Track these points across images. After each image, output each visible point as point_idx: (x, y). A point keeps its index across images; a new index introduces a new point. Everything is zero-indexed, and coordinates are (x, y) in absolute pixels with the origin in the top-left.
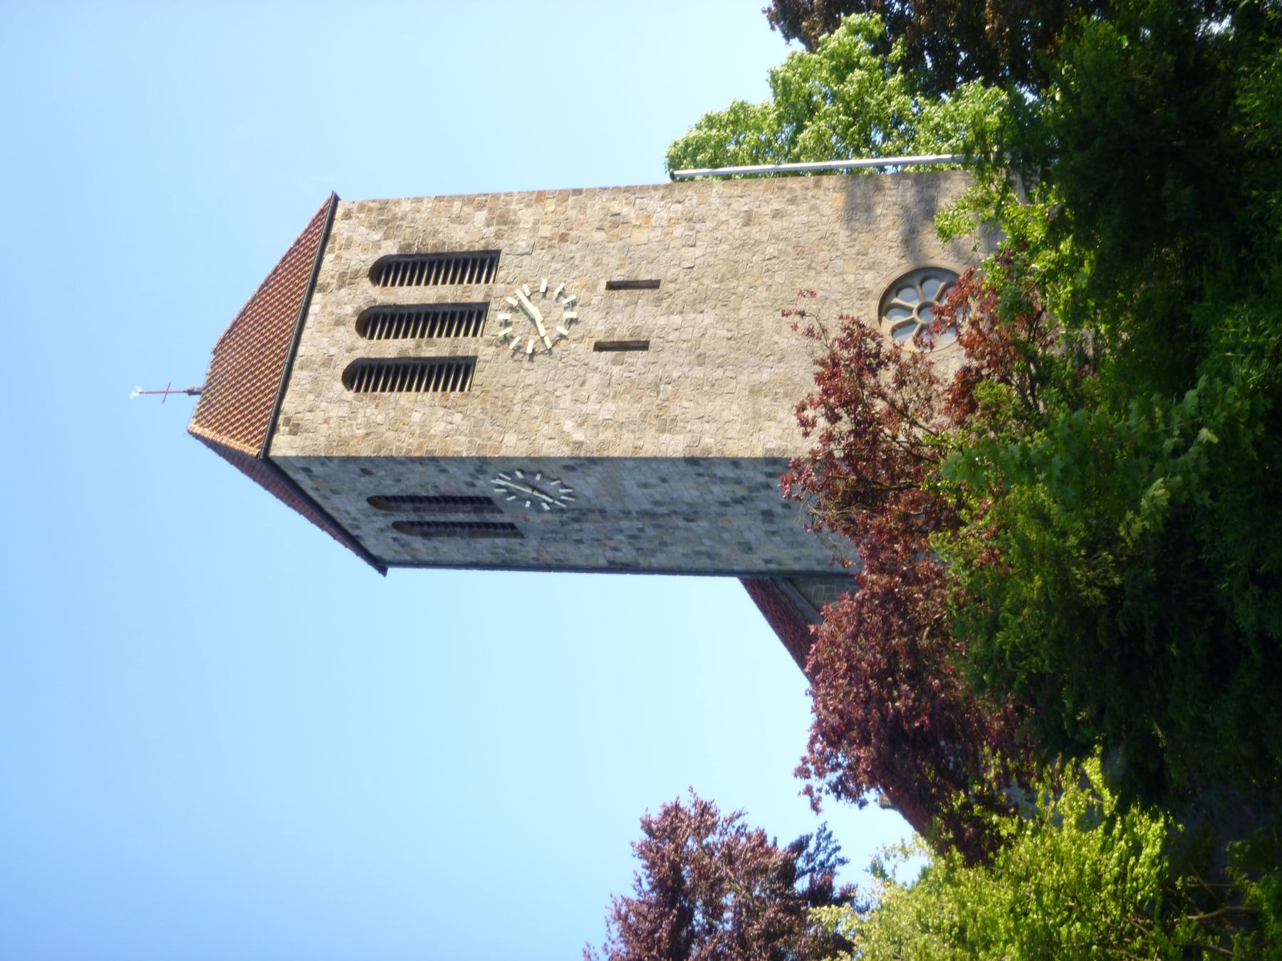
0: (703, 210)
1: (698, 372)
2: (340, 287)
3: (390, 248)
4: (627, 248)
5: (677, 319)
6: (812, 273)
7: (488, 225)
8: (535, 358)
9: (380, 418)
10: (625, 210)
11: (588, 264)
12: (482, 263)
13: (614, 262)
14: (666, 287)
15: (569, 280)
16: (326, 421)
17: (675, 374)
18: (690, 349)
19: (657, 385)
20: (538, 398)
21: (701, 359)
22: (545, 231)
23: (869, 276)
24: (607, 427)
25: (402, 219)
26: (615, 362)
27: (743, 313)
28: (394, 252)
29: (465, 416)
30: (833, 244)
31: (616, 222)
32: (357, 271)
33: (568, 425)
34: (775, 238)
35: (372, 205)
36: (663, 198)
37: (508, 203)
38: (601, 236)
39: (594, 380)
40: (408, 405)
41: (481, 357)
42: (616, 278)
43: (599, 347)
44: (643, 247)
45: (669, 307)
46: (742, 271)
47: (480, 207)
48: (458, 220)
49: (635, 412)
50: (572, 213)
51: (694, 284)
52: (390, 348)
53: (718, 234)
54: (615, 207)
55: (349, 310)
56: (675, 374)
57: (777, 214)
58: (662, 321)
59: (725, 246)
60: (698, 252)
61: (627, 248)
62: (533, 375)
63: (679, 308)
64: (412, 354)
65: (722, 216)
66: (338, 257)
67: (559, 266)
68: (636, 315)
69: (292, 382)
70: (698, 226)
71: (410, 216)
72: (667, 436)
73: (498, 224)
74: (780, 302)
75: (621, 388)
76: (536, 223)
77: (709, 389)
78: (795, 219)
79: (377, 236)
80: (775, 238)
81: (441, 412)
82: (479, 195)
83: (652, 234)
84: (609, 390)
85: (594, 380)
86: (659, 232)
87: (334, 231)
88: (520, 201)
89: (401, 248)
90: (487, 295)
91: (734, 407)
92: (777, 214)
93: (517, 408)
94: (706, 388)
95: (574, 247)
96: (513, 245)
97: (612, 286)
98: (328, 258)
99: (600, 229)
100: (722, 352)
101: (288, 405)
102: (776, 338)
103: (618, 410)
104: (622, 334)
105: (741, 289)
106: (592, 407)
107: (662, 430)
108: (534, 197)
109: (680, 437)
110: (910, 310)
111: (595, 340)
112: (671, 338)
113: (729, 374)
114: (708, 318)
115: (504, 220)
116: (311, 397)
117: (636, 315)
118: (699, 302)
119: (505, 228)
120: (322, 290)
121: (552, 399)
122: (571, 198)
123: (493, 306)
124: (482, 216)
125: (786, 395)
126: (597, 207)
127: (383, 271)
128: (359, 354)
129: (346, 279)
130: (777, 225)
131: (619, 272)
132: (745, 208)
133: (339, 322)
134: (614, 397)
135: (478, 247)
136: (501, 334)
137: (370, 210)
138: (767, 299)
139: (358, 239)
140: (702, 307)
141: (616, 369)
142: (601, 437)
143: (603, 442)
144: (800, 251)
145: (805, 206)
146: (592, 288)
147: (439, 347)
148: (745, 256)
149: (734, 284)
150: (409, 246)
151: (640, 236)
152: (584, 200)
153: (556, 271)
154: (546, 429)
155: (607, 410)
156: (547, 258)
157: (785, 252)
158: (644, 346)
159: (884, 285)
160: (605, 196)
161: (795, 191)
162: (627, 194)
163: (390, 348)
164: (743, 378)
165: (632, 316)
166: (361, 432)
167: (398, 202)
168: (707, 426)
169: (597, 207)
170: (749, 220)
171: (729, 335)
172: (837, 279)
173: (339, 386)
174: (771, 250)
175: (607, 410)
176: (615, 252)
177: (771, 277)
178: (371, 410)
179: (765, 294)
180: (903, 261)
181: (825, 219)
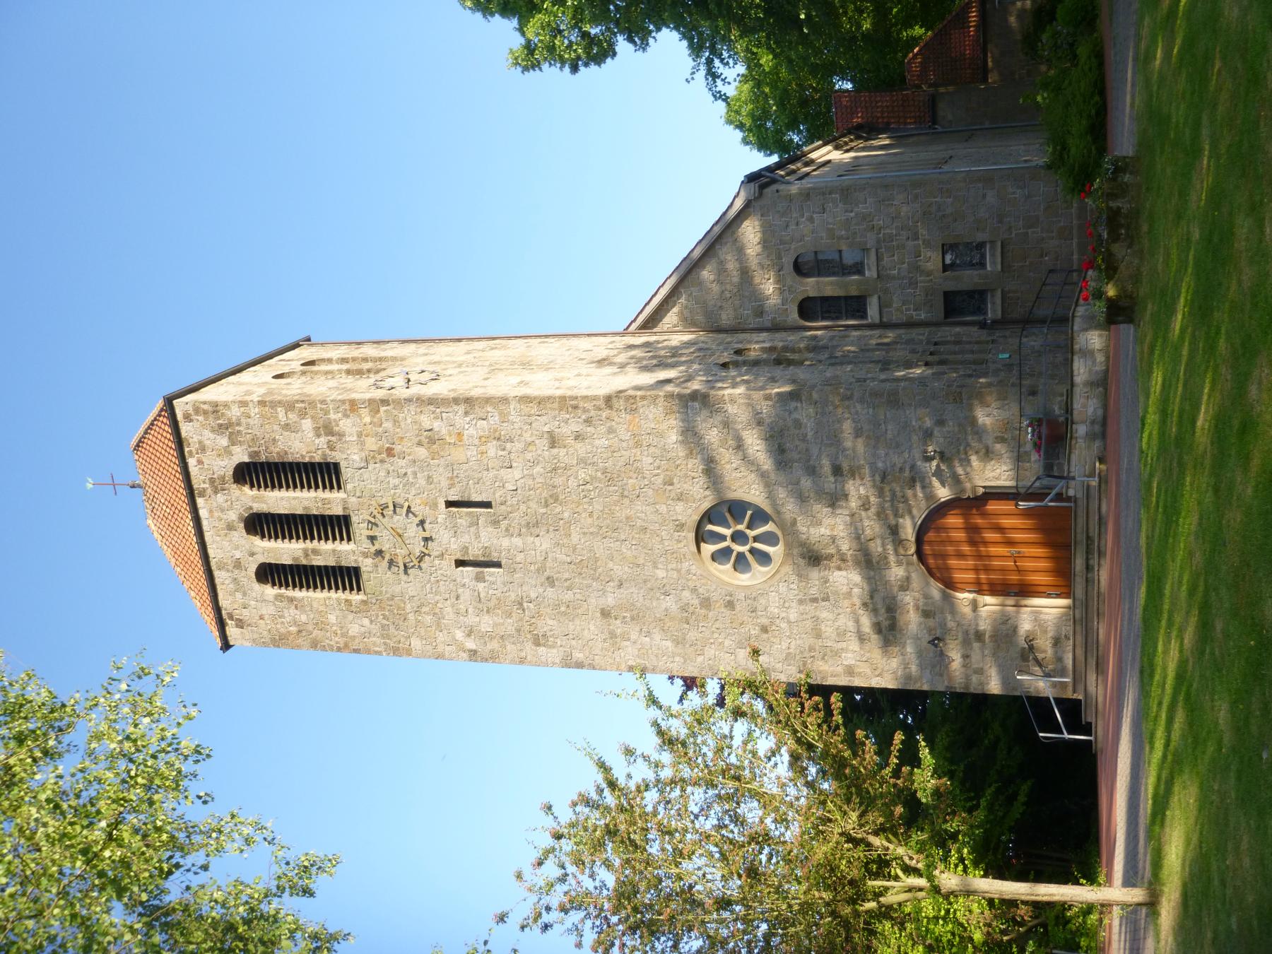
0: (505, 430)
1: (550, 592)
2: (216, 492)
3: (241, 455)
4: (451, 466)
5: (517, 541)
6: (626, 501)
7: (319, 436)
8: (410, 571)
9: (304, 618)
10: (436, 425)
11: (422, 482)
12: (324, 473)
13: (445, 483)
14: (498, 510)
15: (411, 498)
16: (261, 618)
17: (533, 595)
18: (538, 570)
19: (521, 604)
20: (424, 609)
21: (551, 581)
22: (371, 444)
23: (680, 507)
24: (492, 638)
25: (239, 424)
26: (479, 578)
27: (575, 538)
28: (246, 459)
29: (371, 622)
30: (639, 471)
31: (432, 439)
32: (223, 477)
33: (459, 635)
34: (583, 461)
35: (205, 407)
36: (466, 413)
37: (327, 413)
38: (422, 452)
39: (466, 595)
40: (321, 608)
41: (363, 569)
42: (451, 498)
43: (460, 563)
44: (465, 467)
45: (507, 530)
46: (562, 497)
47: (303, 414)
48: (287, 427)
49: (509, 625)
50: (388, 425)
51: (523, 507)
52: (287, 551)
53: (529, 456)
54: (426, 421)
55: (233, 516)
56: (533, 595)
57: (578, 437)
58: (505, 542)
59: (538, 469)
60: (517, 474)
61: (451, 466)
62: (411, 586)
63: (517, 531)
64: (304, 562)
65: (527, 437)
66: (200, 462)
67: (397, 481)
68: (481, 536)
69: (217, 581)
70: (508, 445)
71: (243, 420)
72: (542, 650)
73: (327, 435)
74: (604, 530)
75: (491, 604)
76: (360, 435)
77: (567, 611)
78: (597, 442)
79: (224, 441)
80: (583, 461)
81: (351, 617)
82: (297, 401)
83: (469, 453)
84: (483, 606)
85: (466, 595)
86: (472, 452)
87: (184, 434)
88: (337, 410)
89: (250, 456)
90: (344, 509)
91: (592, 628)
92: (578, 437)
93: (411, 616)
94: (563, 609)
95: (402, 463)
96: (349, 458)
97: (450, 504)
98: (192, 462)
99: (420, 444)
100: (566, 575)
101: (224, 602)
102: (611, 565)
103: (496, 625)
104: (474, 553)
105: (566, 515)
106: (472, 619)
107: (537, 644)
108: (347, 406)
109: (555, 651)
110: (723, 538)
111: (454, 558)
112: (518, 559)
113: (578, 596)
114: (544, 543)
115: (327, 429)
116: (239, 595)
117: (481, 536)
118: (532, 526)
119: (333, 439)
120: (202, 494)
121: (437, 611)
122: (383, 409)
123: (354, 519)
124: (307, 424)
125: (633, 619)
126: (409, 420)
127: (247, 473)
128: (262, 559)
129: (217, 485)
130: (581, 448)
131: (452, 491)
132: (546, 429)
133: (230, 527)
134: (488, 612)
135: (318, 459)
136: (373, 549)
137: (205, 412)
138: (592, 525)
139: (207, 443)
140: (536, 531)
141: (481, 586)
142: (489, 647)
143: (492, 651)
144: (610, 478)
145: (603, 429)
146: (434, 506)
147: (326, 552)
148: (559, 481)
149: (559, 509)
150: (257, 453)
151: (458, 454)
152: (395, 412)
153: (395, 487)
154: (441, 637)
155: (486, 623)
156: (382, 474)
157: (593, 478)
158: (498, 565)
159: (697, 518)
160: (412, 408)
161: (588, 411)
162: (432, 408)
163: (287, 551)
164: (593, 601)
165: (477, 536)
166: (293, 629)
167: (226, 405)
168: (574, 642)
169: (409, 420)
170: (553, 442)
171: (569, 560)
172: (650, 509)
173: (257, 587)
174: (582, 474)
175: (486, 623)
176: (441, 469)
177: (590, 503)
178: (293, 611)
179: (589, 521)
180: (707, 493)
181: (624, 444)
